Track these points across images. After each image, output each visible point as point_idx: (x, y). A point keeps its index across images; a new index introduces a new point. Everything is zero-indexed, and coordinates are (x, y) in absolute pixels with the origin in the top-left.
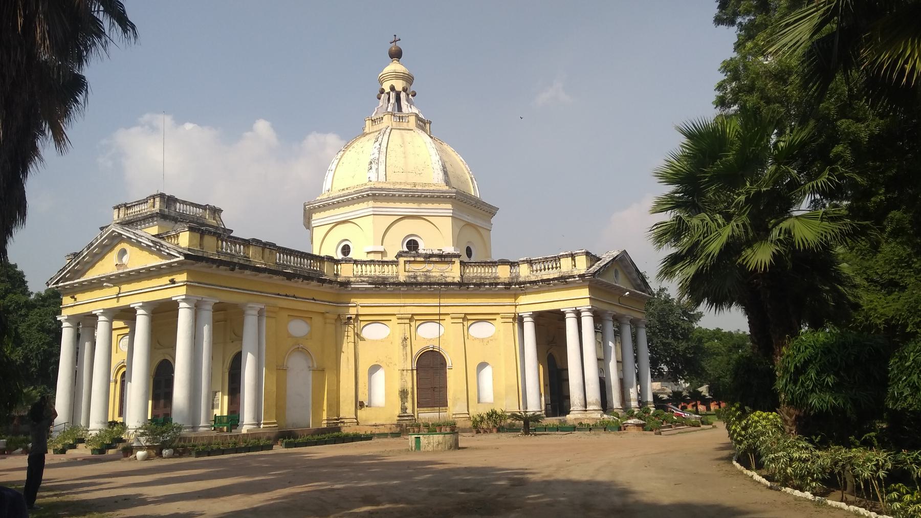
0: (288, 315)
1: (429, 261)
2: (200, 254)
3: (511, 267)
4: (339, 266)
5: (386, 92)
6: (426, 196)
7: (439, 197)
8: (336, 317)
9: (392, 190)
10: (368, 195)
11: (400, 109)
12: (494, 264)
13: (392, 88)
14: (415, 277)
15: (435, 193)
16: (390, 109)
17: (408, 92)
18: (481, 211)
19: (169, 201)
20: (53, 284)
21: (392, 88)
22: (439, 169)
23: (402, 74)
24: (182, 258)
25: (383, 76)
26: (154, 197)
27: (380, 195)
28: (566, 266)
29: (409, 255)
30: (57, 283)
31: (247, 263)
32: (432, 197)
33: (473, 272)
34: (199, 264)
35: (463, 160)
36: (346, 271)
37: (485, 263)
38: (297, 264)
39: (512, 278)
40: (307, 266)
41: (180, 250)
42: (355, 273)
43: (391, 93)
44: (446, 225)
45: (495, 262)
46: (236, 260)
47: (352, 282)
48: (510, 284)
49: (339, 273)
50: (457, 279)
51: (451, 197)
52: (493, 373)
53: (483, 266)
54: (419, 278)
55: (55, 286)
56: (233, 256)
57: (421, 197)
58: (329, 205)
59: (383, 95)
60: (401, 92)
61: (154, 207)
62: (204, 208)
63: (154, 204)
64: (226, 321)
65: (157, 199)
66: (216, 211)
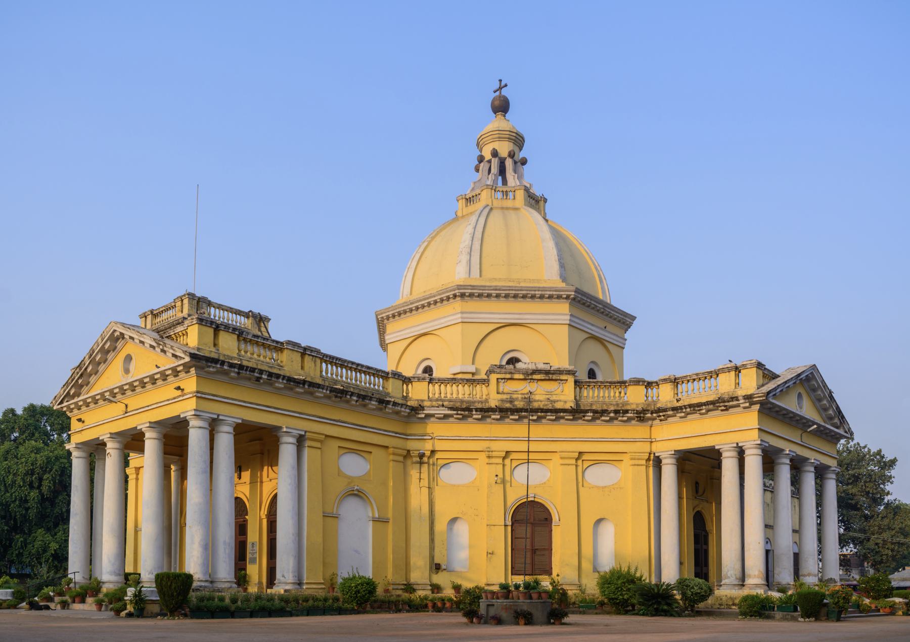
0: (339, 447)
1: (531, 379)
3: (647, 389)
4: (410, 386)
5: (486, 159)
7: (550, 297)
8: (405, 453)
11: (505, 182)
12: (623, 384)
13: (495, 154)
14: (511, 401)
16: (489, 182)
17: (516, 158)
19: (199, 302)
20: (58, 405)
21: (495, 154)
25: (483, 137)
28: (725, 385)
29: (503, 370)
30: (61, 402)
33: (593, 396)
36: (418, 392)
38: (351, 380)
39: (649, 405)
40: (365, 383)
42: (431, 395)
43: (493, 159)
44: (561, 336)
47: (426, 406)
48: (644, 411)
49: (410, 395)
50: (570, 405)
52: (616, 534)
54: (516, 403)
55: (59, 406)
59: (482, 164)
60: (506, 158)
61: (182, 312)
63: (182, 308)
64: (263, 454)
65: (186, 301)
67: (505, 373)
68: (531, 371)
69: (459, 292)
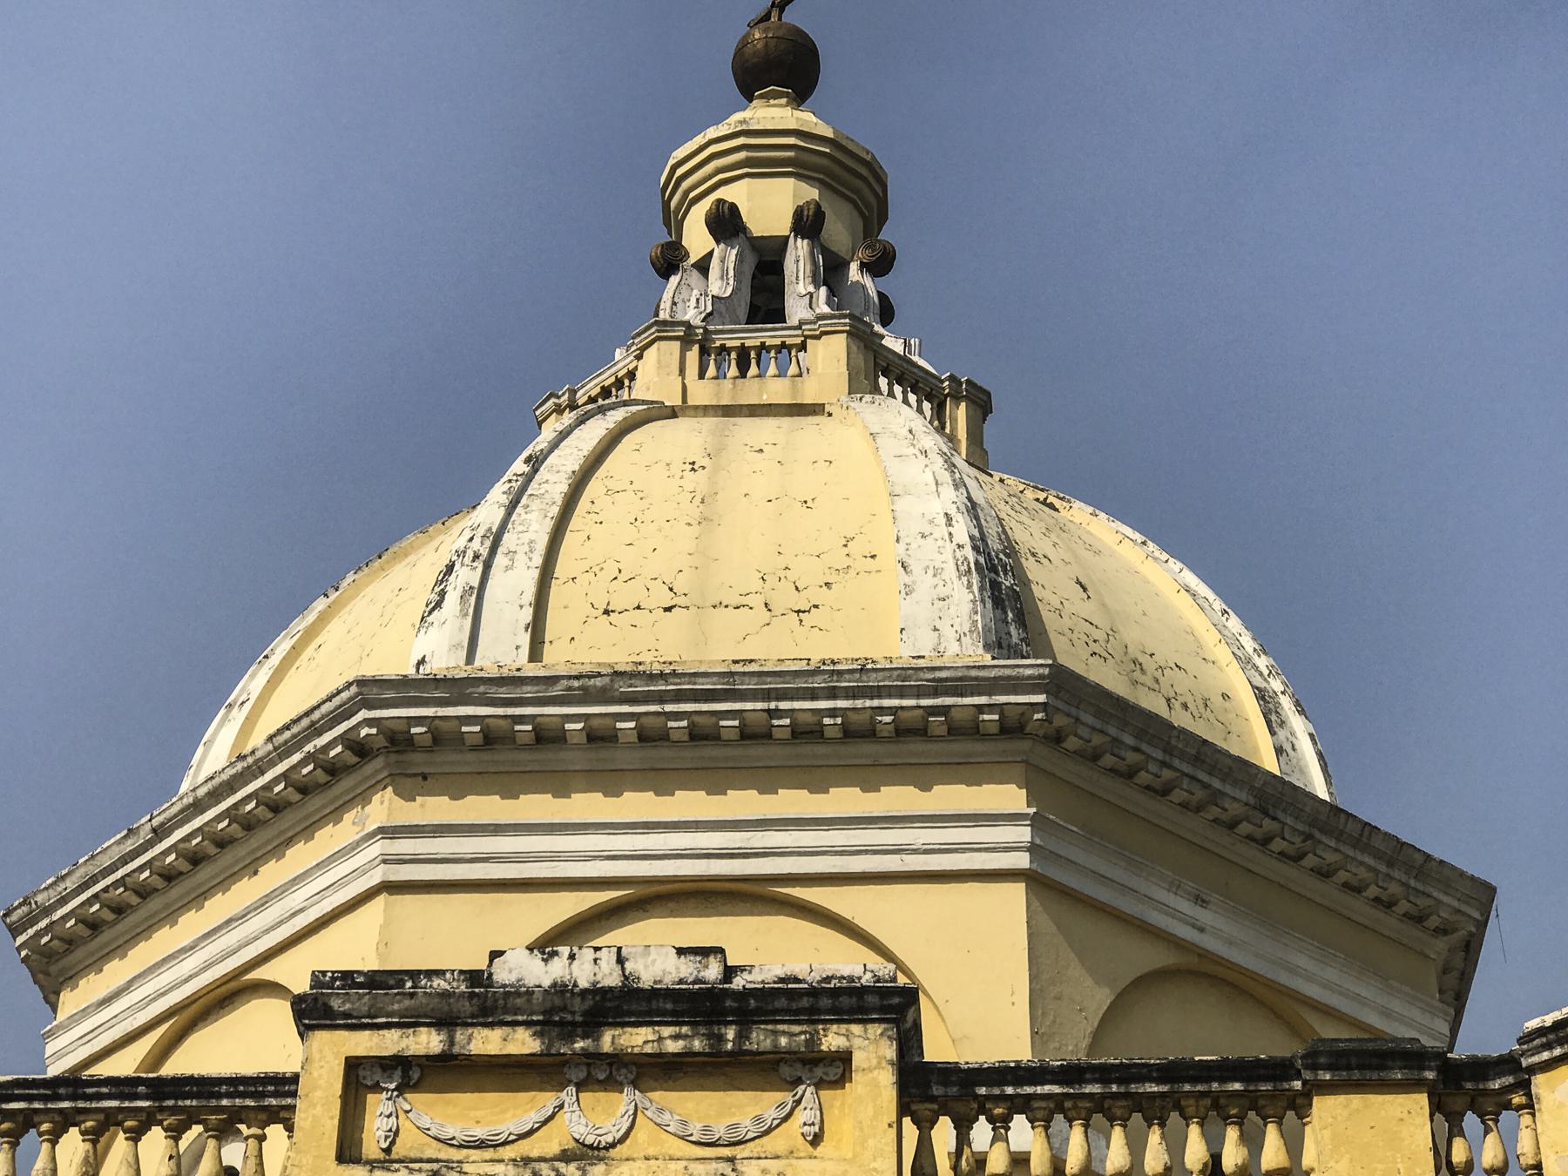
6: (807, 732)
7: (909, 730)
9: (528, 691)
10: (360, 749)
13: (726, 223)
15: (878, 692)
18: (1327, 892)
22: (950, 571)
23: (791, 141)
27: (442, 737)
32: (857, 732)
35: (1203, 589)
37: (1172, 1072)
45: (1279, 1070)
51: (1013, 727)
53: (1155, 1112)
57: (766, 735)
58: (144, 892)
67: (409, 1022)
68: (589, 1003)
69: (368, 722)
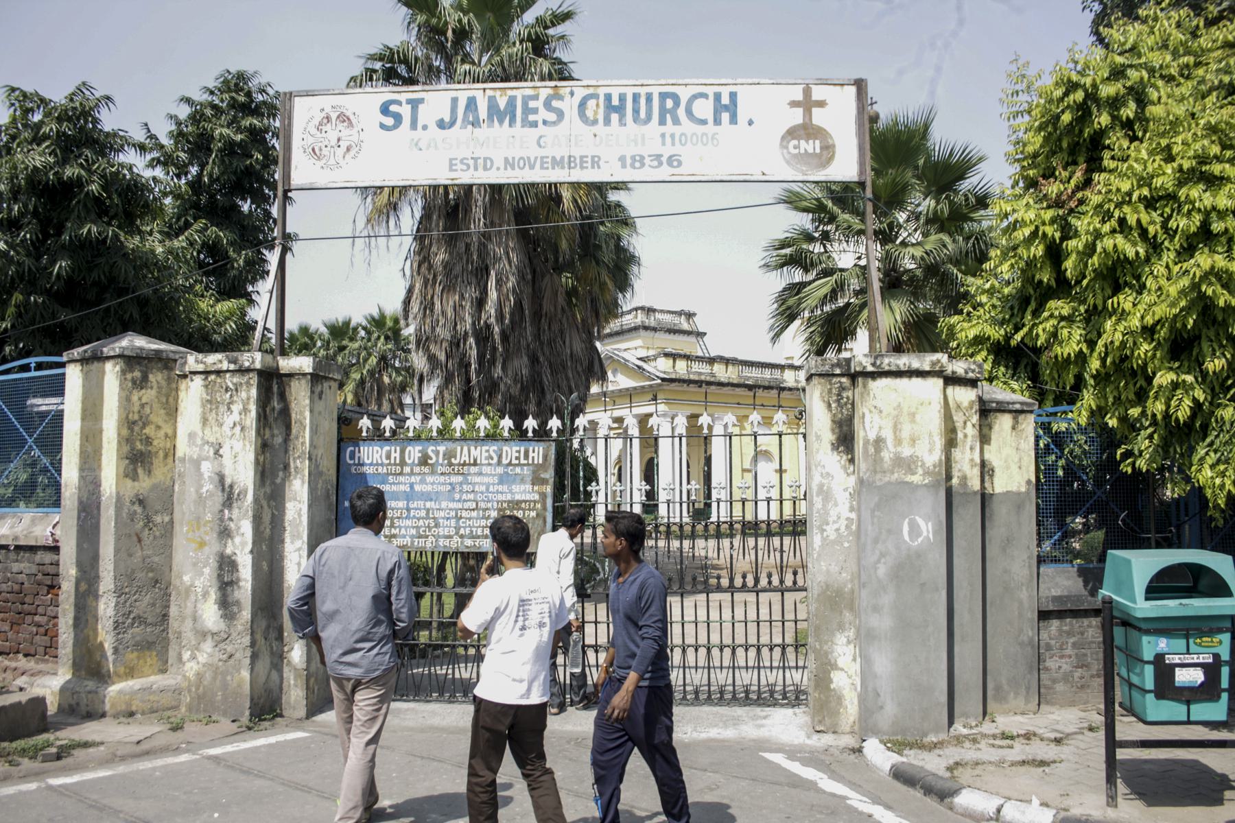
2: (673, 376)
19: (650, 311)
24: (659, 381)
26: (636, 309)
31: (712, 379)
34: (673, 384)
41: (658, 374)
46: (703, 378)
56: (700, 374)
62: (680, 313)
66: (690, 316)
